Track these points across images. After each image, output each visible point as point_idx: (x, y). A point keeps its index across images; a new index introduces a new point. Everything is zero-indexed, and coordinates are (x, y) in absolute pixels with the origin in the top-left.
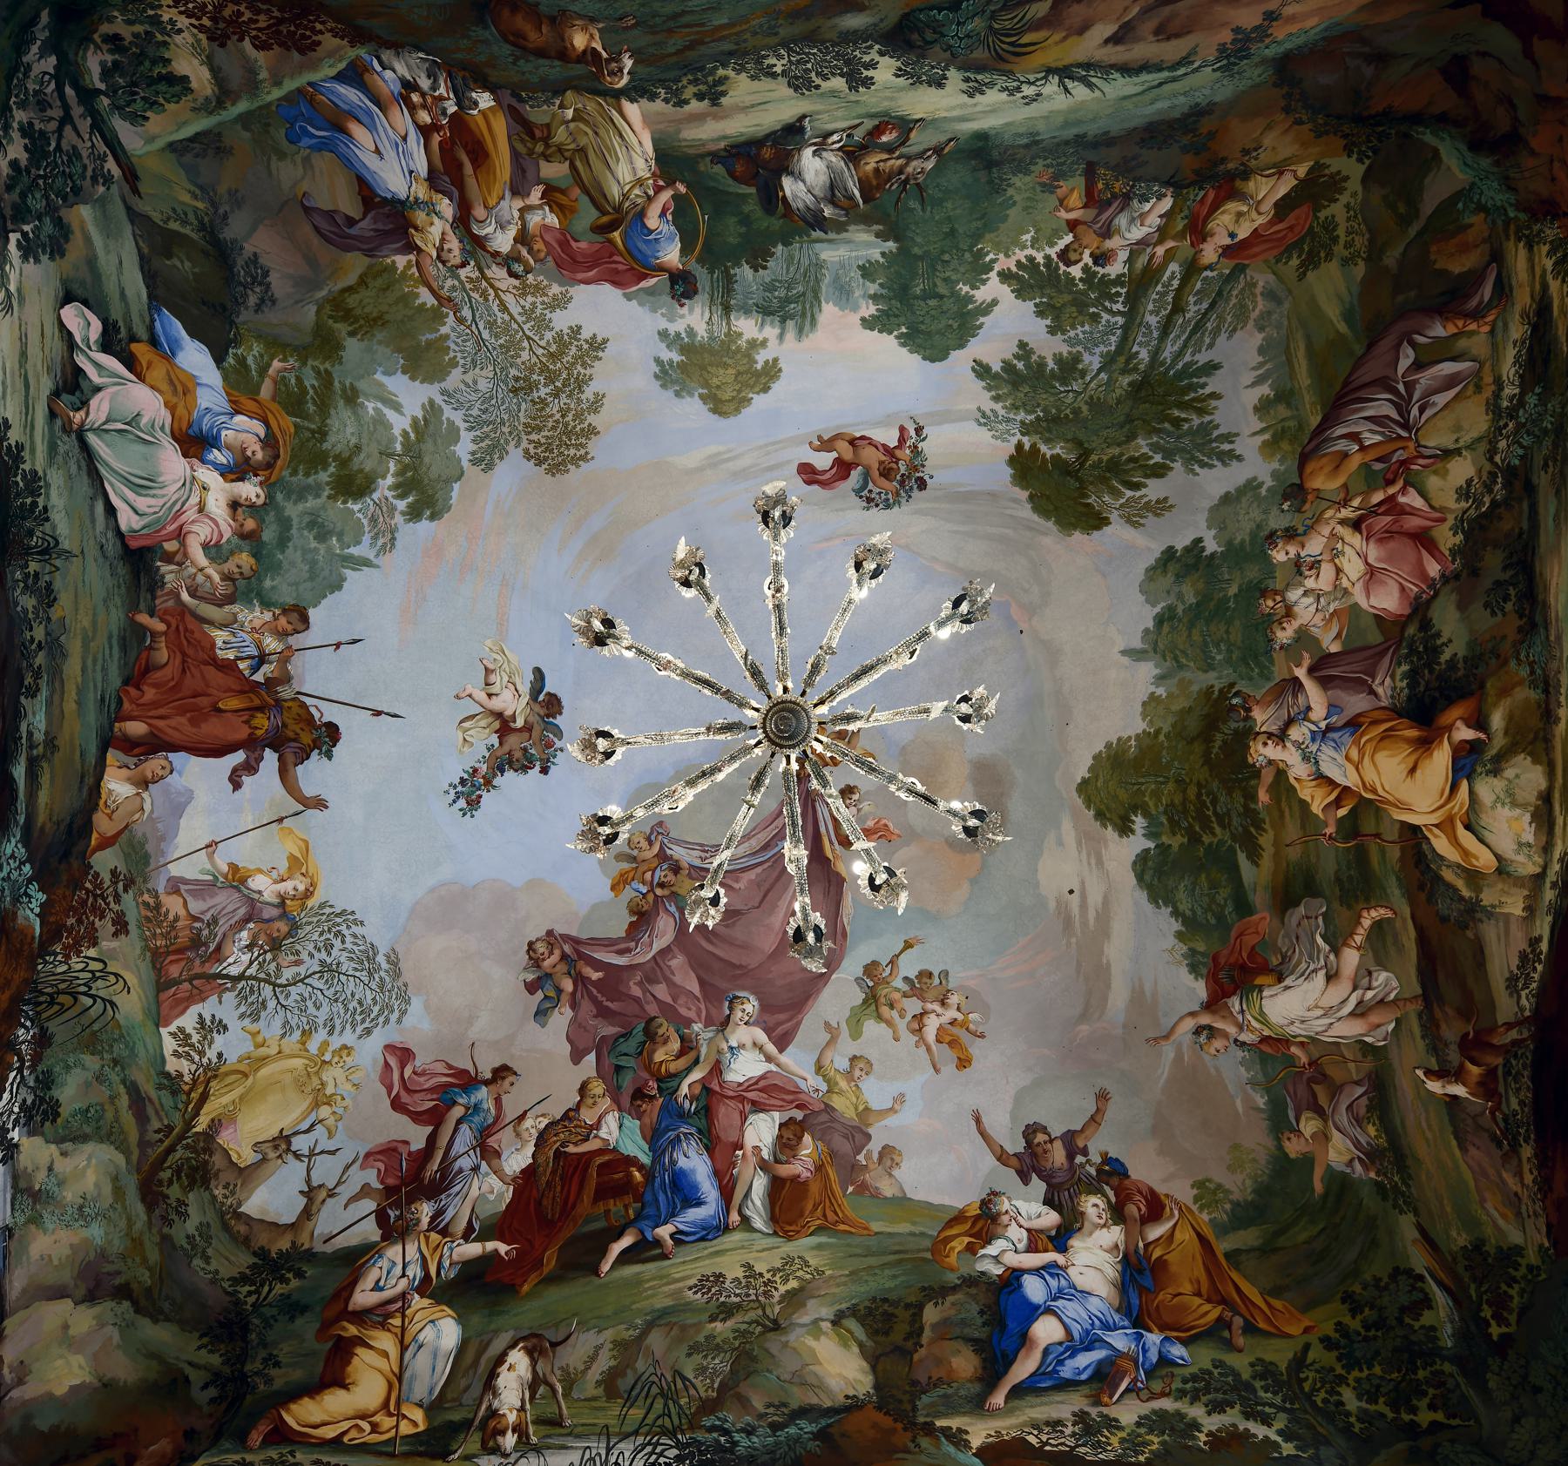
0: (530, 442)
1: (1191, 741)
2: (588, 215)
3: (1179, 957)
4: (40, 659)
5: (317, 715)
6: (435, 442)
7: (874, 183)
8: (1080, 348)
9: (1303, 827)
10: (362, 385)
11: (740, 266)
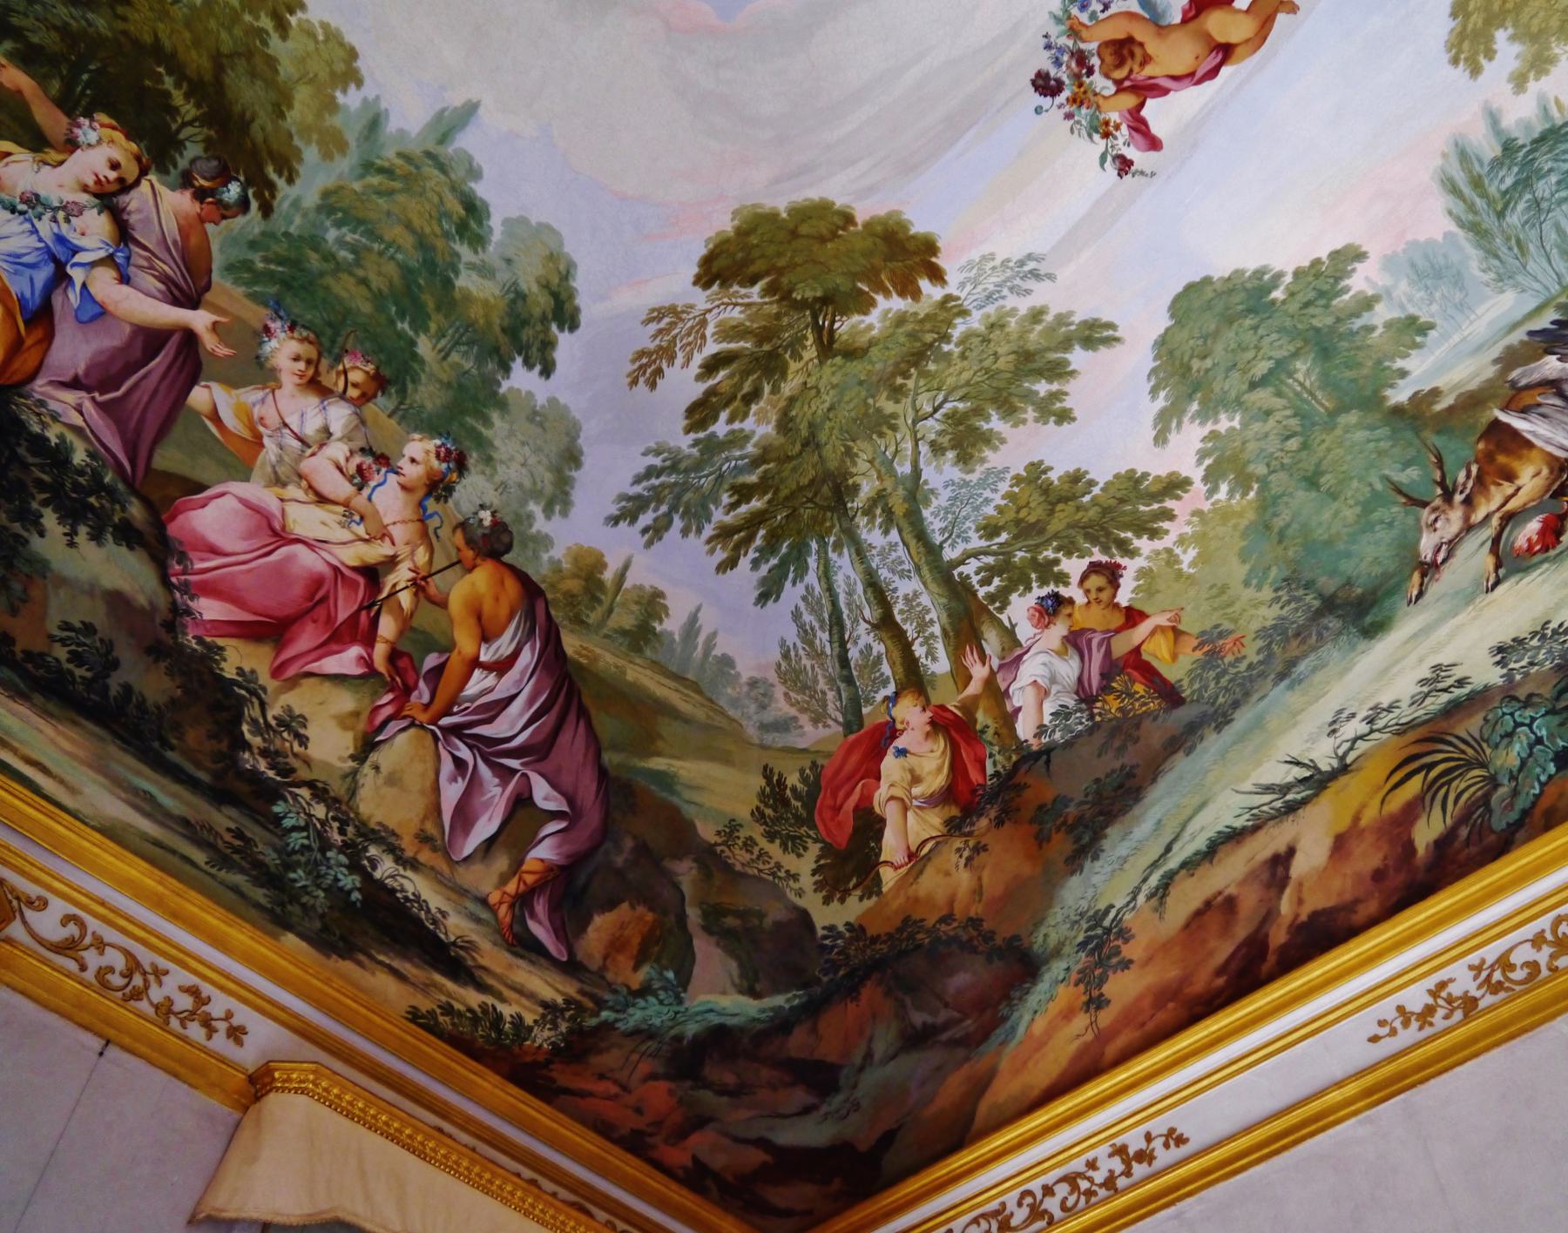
7: (1502, 459)
8: (974, 478)
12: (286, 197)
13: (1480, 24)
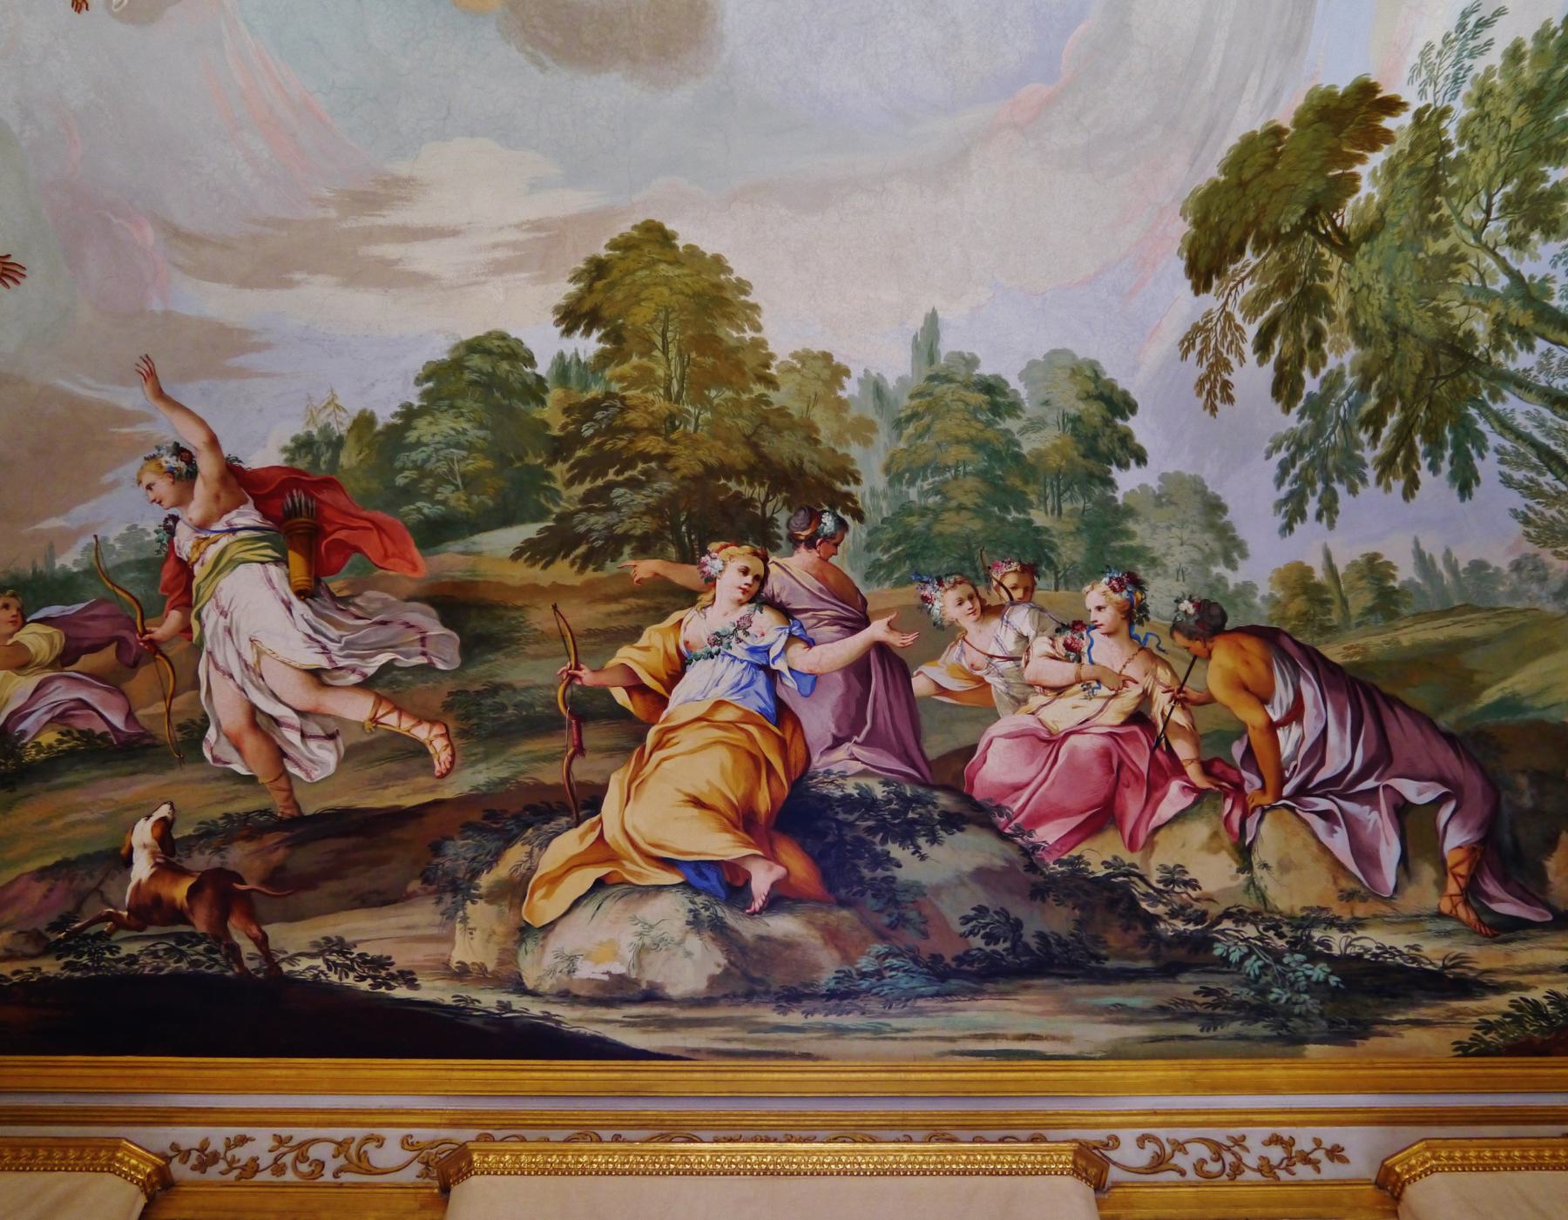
1: (751, 443)
3: (322, 419)
9: (591, 633)
12: (863, 495)
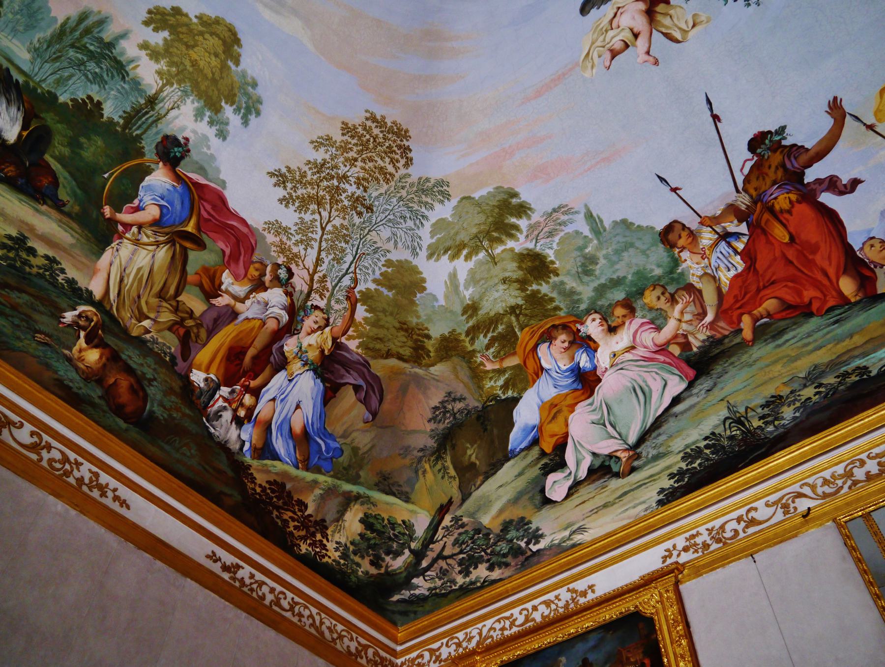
0: (397, 169)
2: (197, 259)
4: (830, 380)
5: (749, 165)
6: (457, 233)
10: (458, 309)
11: (111, 121)
13: (171, 22)
